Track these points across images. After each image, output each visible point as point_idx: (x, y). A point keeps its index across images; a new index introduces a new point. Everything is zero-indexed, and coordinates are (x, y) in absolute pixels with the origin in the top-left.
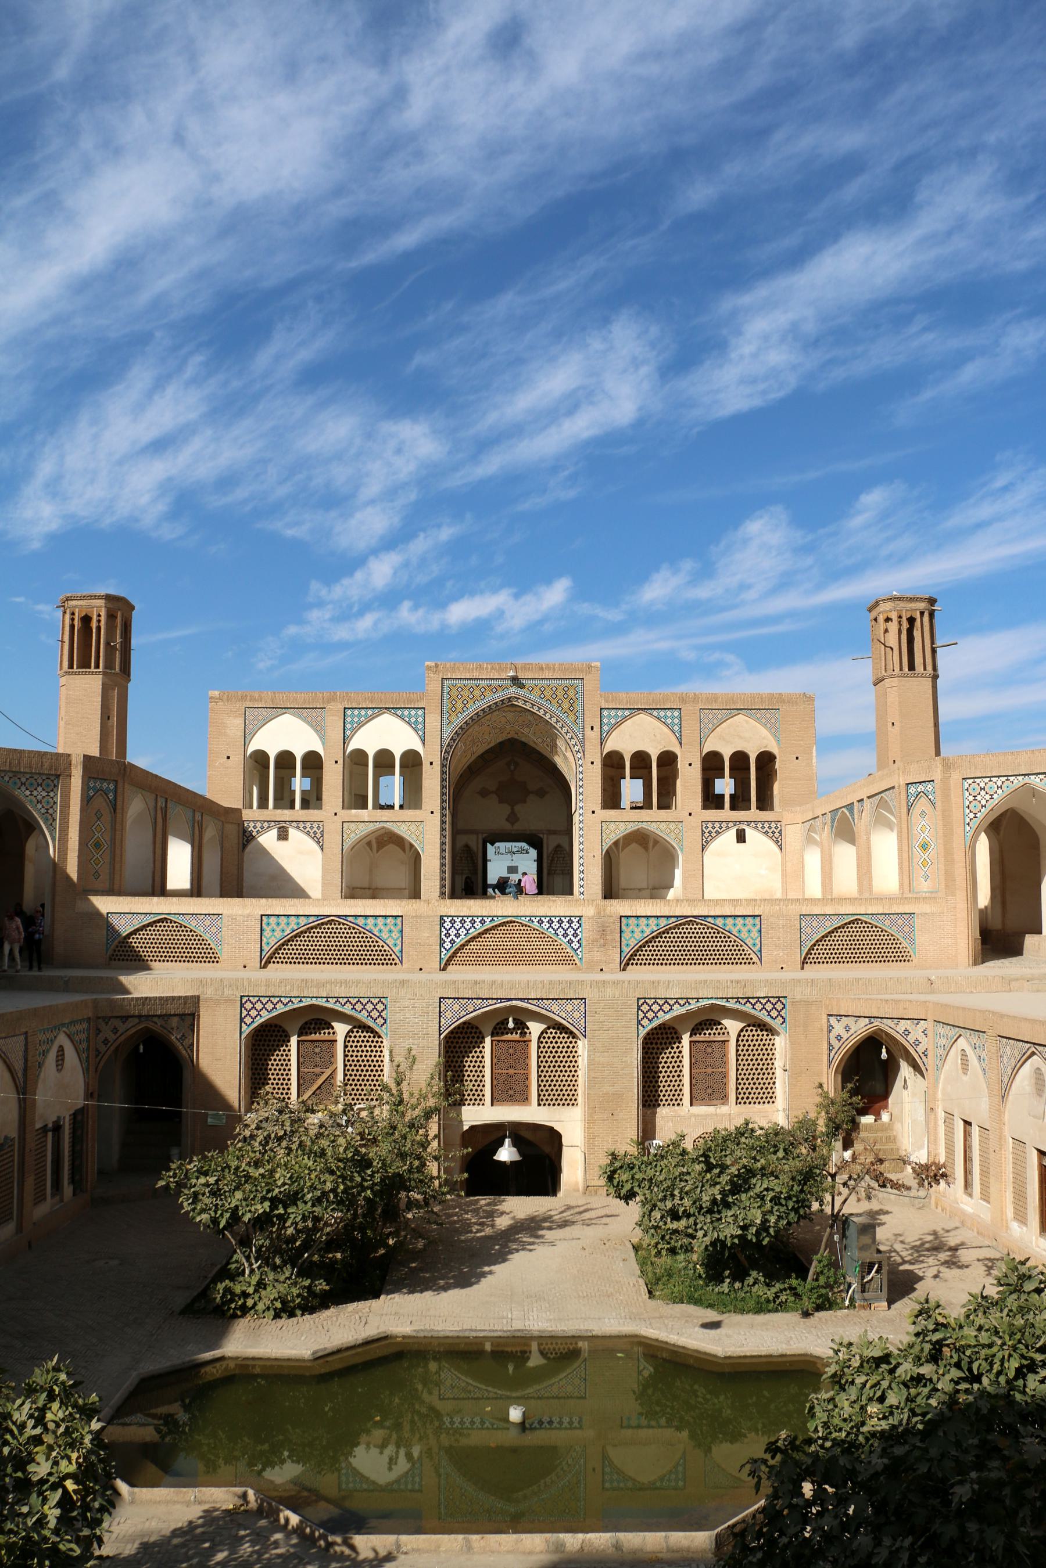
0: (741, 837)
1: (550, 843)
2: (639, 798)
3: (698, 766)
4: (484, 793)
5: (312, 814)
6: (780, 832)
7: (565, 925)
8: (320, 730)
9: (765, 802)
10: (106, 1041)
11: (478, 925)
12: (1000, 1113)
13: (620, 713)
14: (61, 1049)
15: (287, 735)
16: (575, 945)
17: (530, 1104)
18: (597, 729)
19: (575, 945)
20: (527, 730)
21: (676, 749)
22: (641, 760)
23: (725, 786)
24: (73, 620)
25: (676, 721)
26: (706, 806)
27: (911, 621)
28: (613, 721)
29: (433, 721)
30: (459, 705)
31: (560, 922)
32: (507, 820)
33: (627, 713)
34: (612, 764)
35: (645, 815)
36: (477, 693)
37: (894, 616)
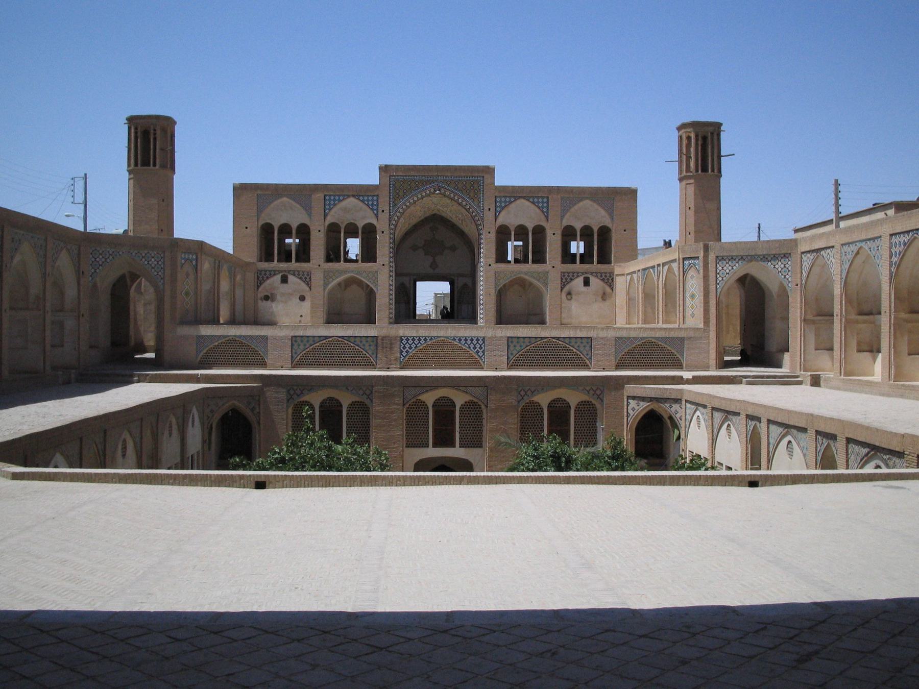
0: (587, 283)
1: (460, 282)
4: (415, 248)
5: (304, 265)
9: (604, 258)
10: (212, 411)
11: (422, 342)
13: (508, 199)
15: (287, 214)
16: (481, 354)
18: (493, 210)
19: (481, 354)
20: (445, 209)
21: (544, 224)
22: (521, 232)
23: (578, 247)
24: (136, 133)
25: (545, 205)
26: (564, 262)
27: (705, 138)
28: (503, 205)
29: (384, 204)
30: (401, 194)
31: (472, 340)
33: (512, 199)
34: (503, 234)
35: (522, 267)
36: (413, 185)
37: (693, 136)
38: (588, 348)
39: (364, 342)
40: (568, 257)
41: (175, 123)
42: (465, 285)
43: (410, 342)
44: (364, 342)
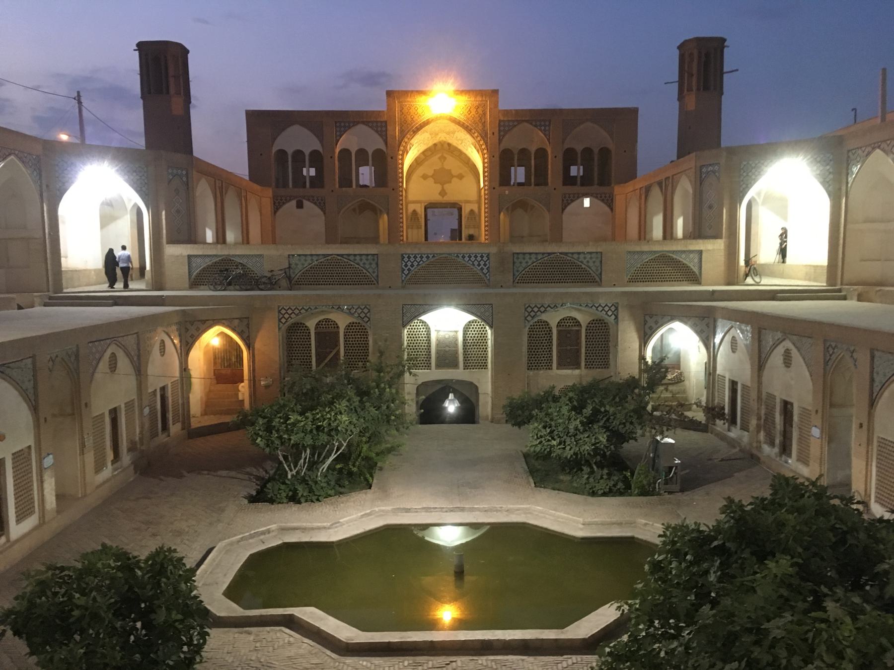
2: (521, 178)
3: (560, 156)
4: (425, 177)
6: (612, 200)
7: (479, 259)
8: (320, 136)
9: (605, 180)
11: (424, 259)
12: (760, 376)
14: (163, 342)
16: (485, 271)
17: (781, 399)
19: (485, 271)
26: (564, 184)
27: (707, 55)
28: (507, 129)
31: (476, 257)
32: (440, 194)
38: (598, 264)
39: (364, 261)
40: (569, 180)
41: (188, 52)
42: (472, 211)
43: (412, 259)
44: (364, 261)
